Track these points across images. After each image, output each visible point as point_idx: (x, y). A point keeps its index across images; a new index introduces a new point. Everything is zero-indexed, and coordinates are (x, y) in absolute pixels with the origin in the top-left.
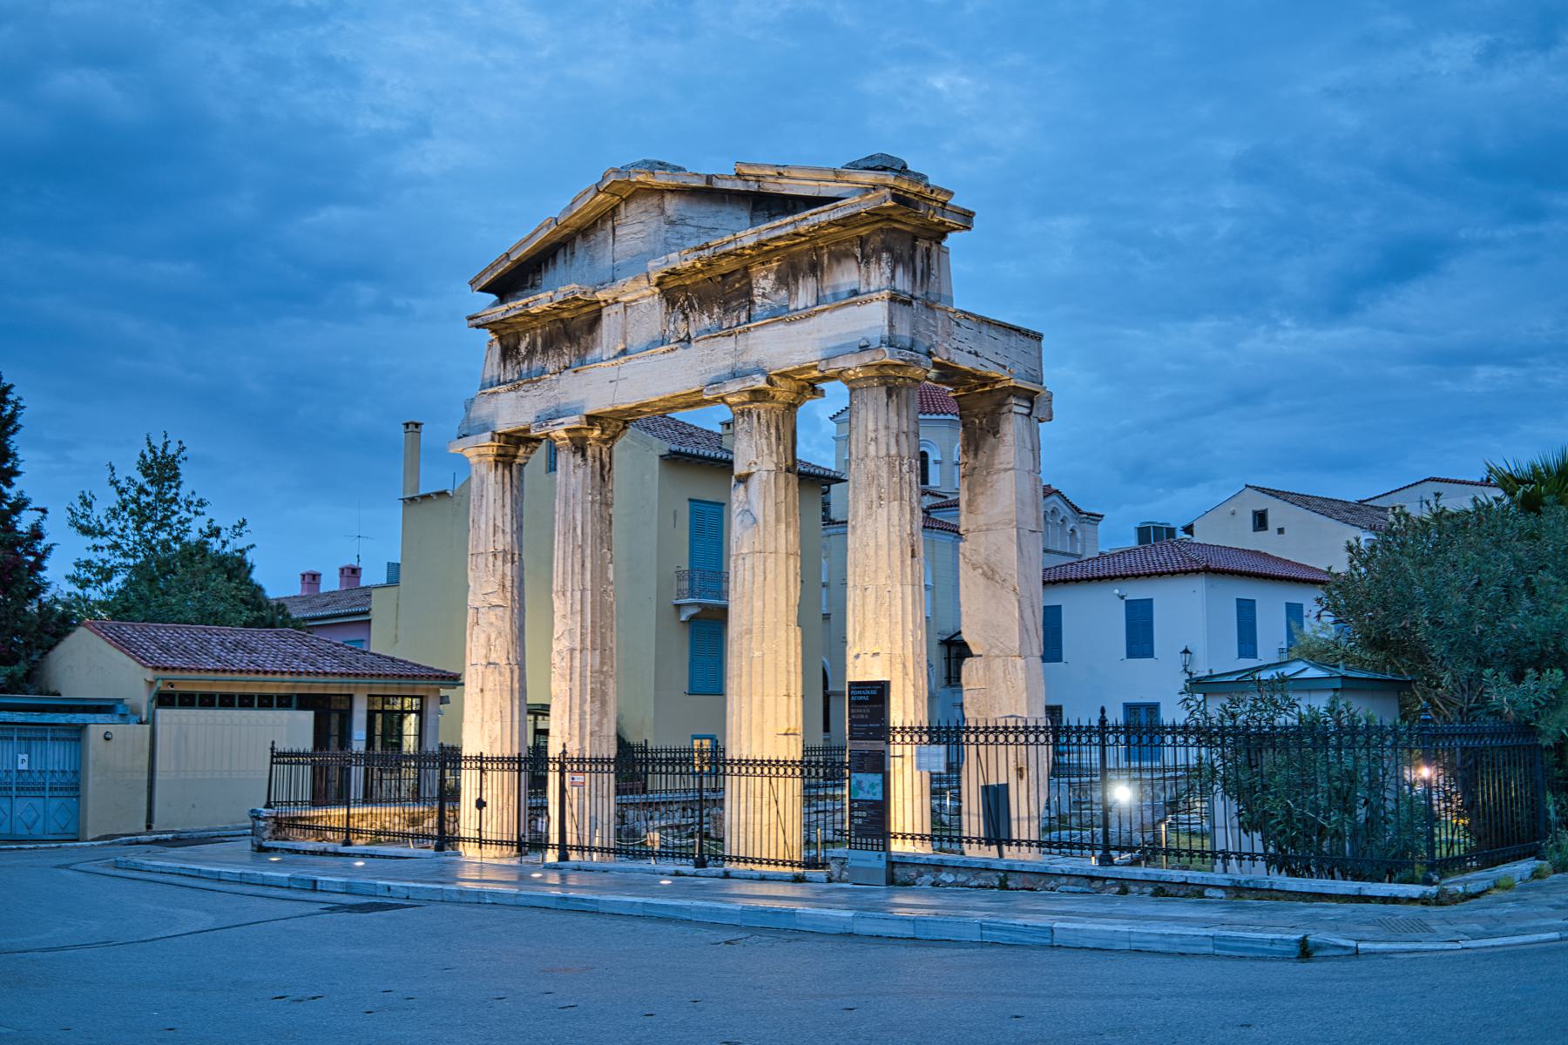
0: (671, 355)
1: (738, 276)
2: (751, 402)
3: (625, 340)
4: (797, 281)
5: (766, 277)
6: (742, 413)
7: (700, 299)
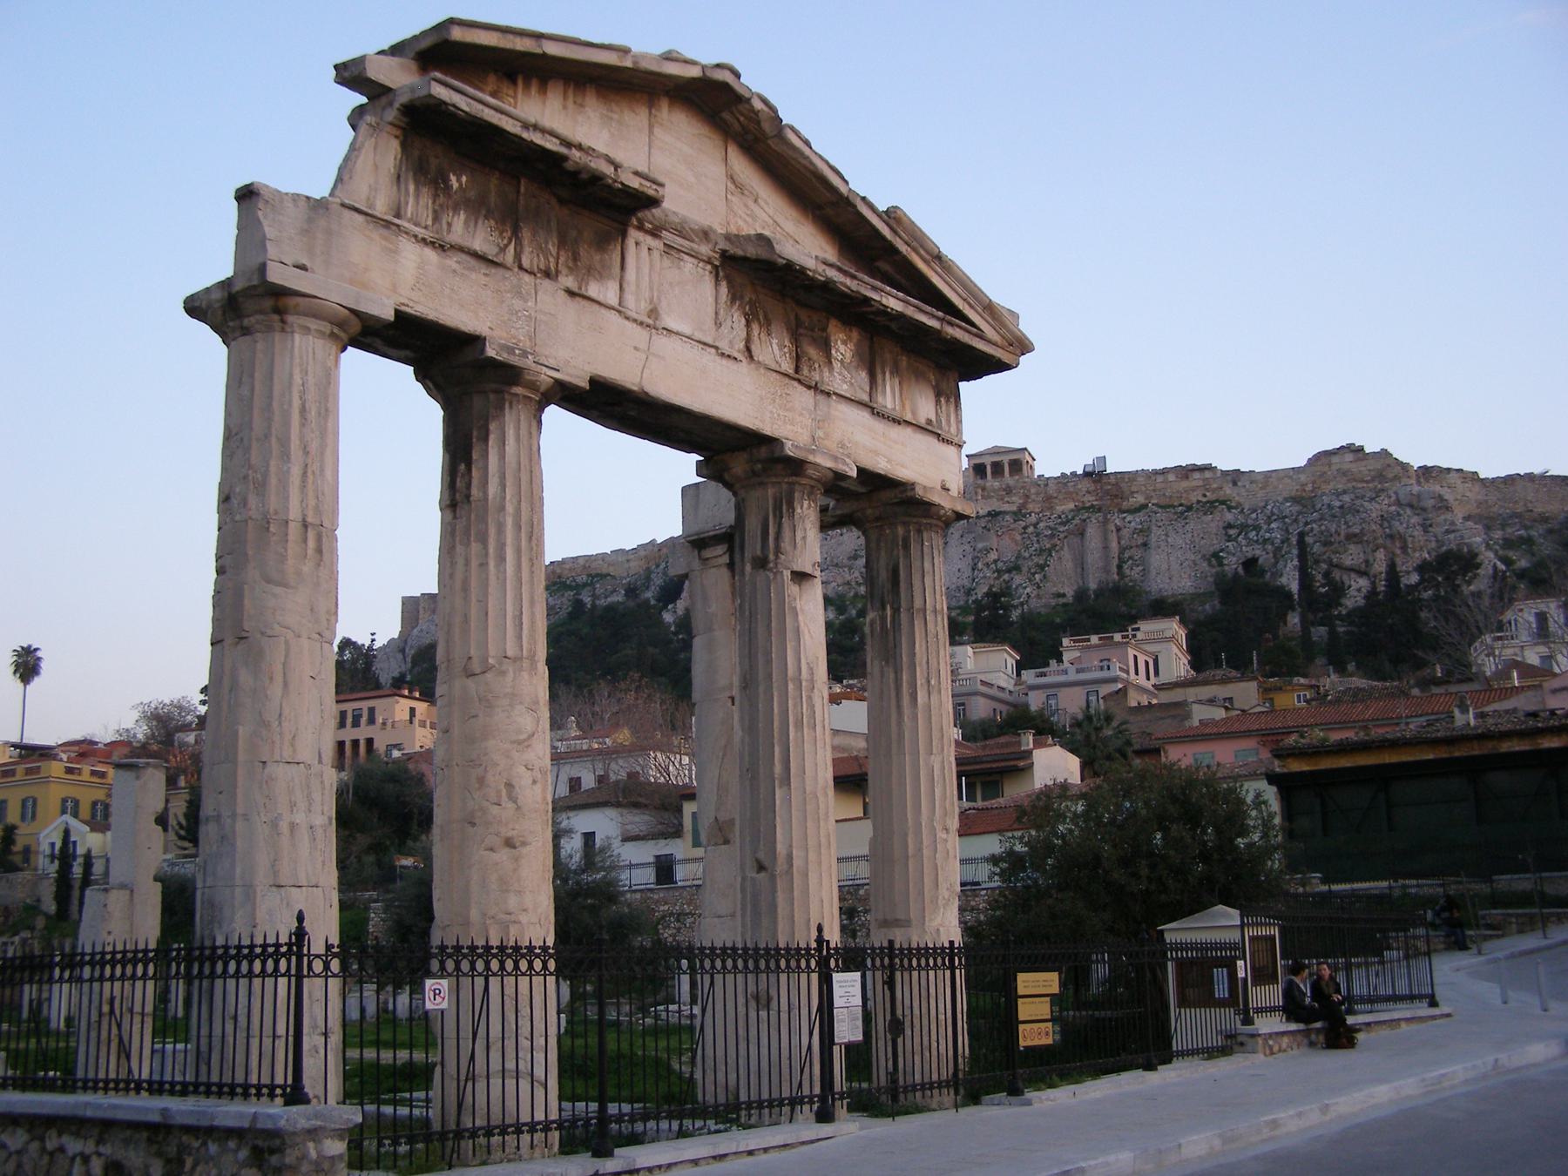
0: (730, 363)
4: (884, 373)
5: (844, 343)
7: (766, 317)
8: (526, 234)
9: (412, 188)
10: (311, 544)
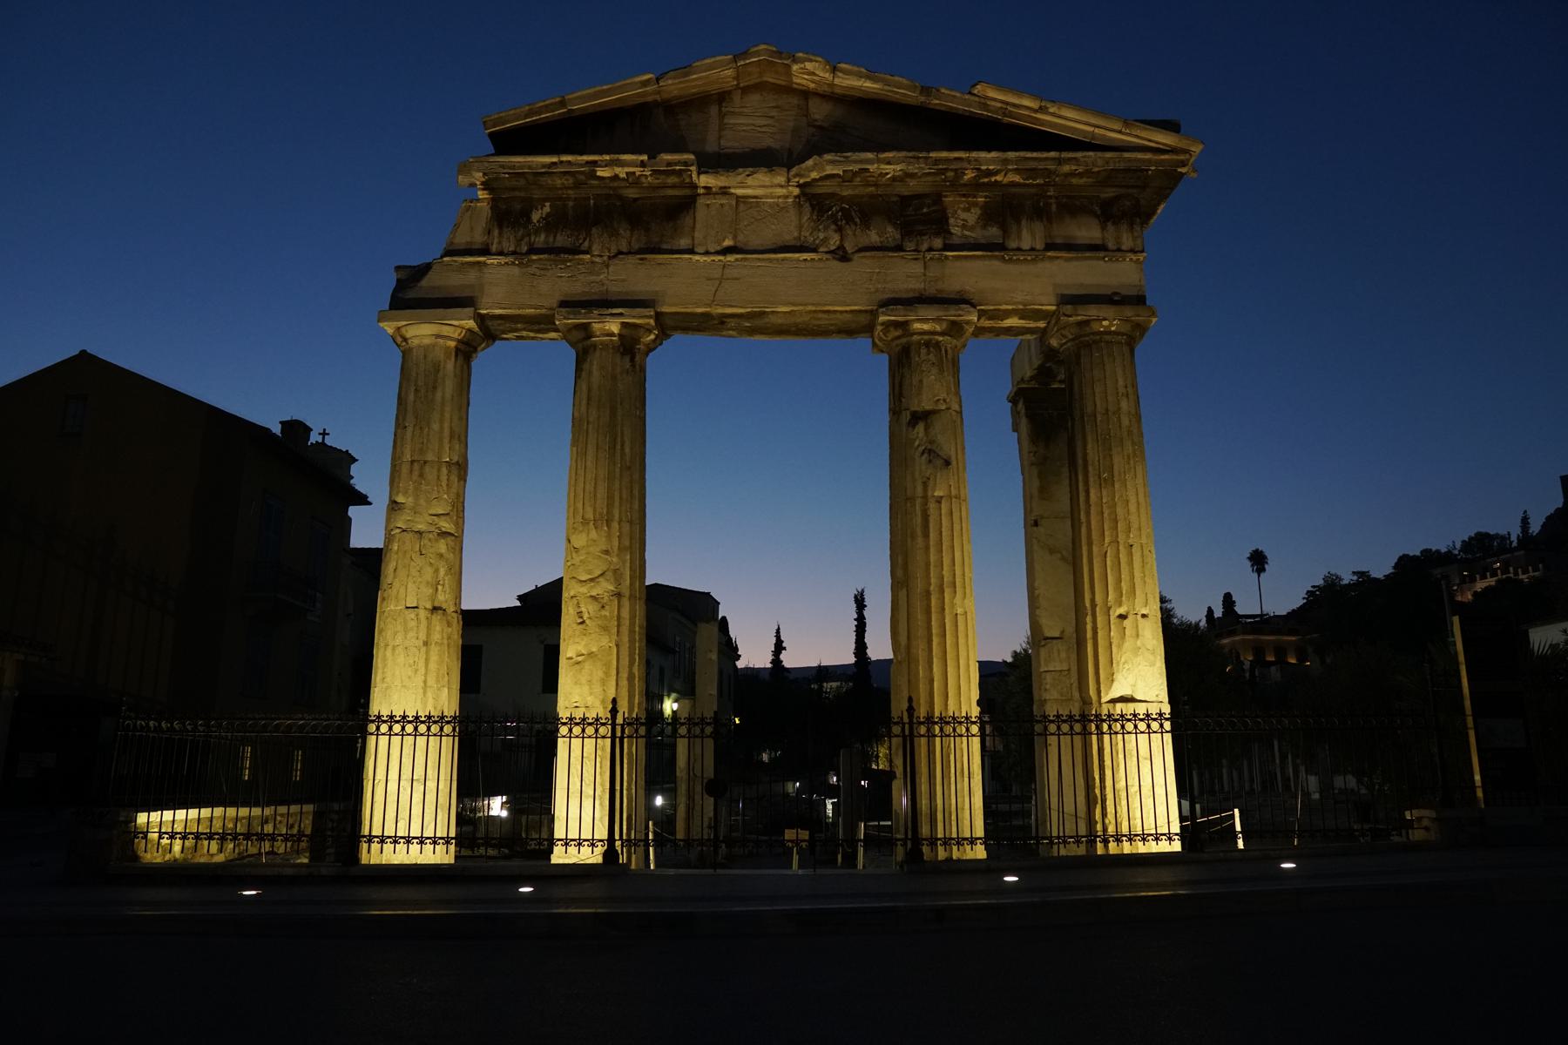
1: (928, 201)
2: (942, 334)
3: (735, 237)
4: (1019, 222)
5: (967, 210)
6: (927, 344)
8: (594, 230)
9: (496, 232)
10: (416, 473)
